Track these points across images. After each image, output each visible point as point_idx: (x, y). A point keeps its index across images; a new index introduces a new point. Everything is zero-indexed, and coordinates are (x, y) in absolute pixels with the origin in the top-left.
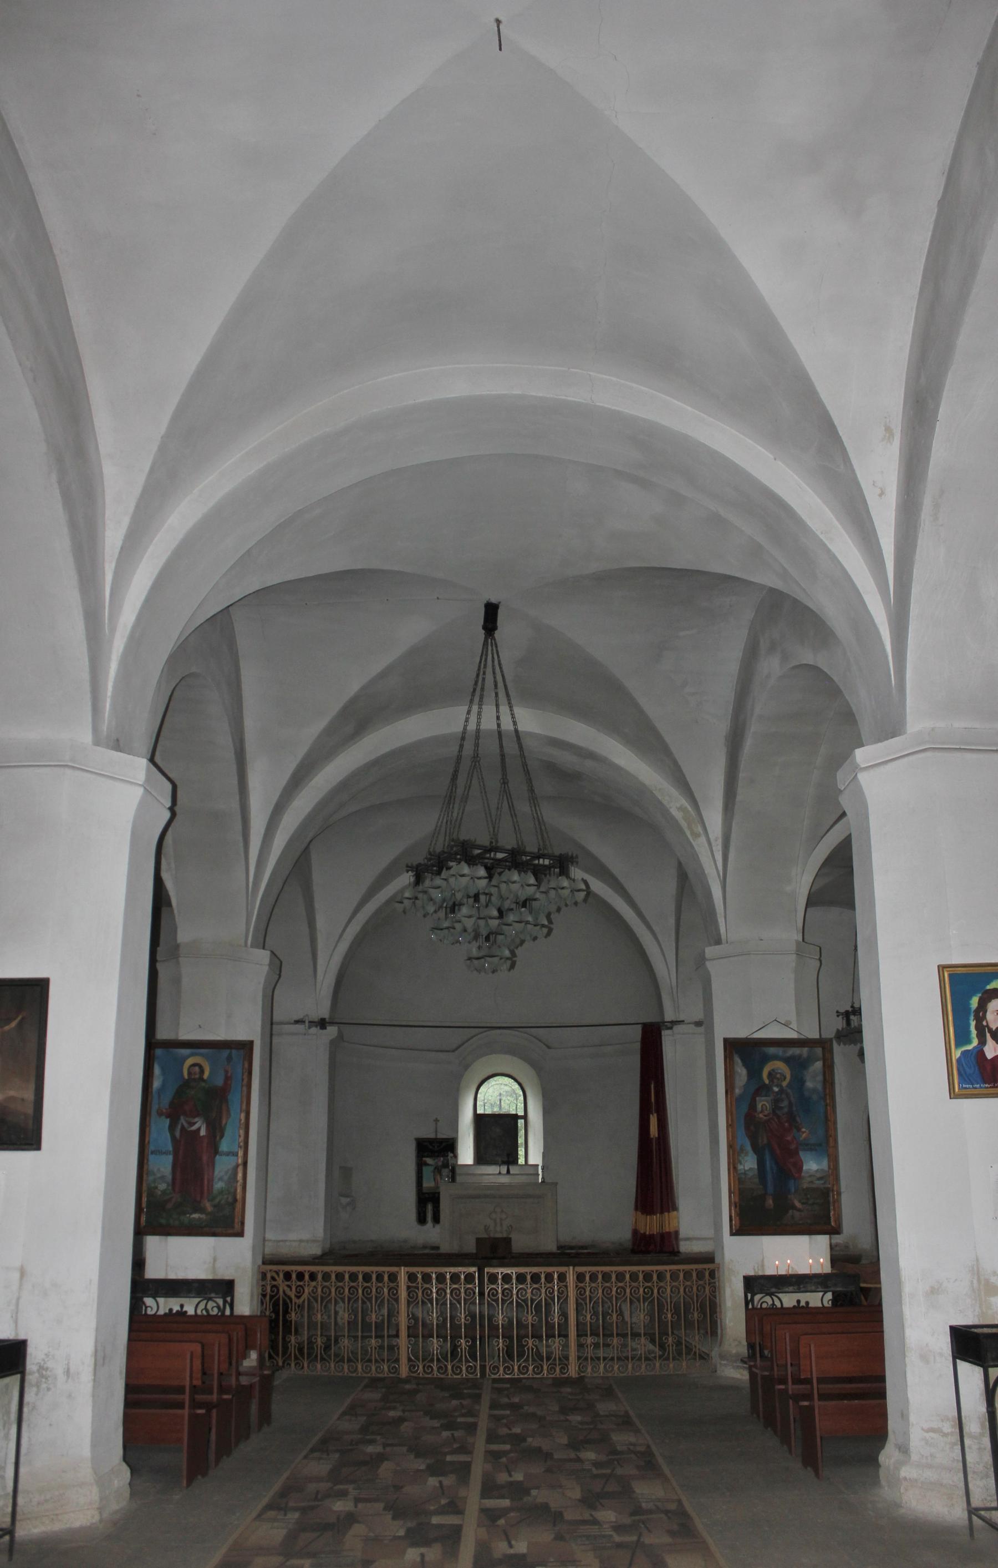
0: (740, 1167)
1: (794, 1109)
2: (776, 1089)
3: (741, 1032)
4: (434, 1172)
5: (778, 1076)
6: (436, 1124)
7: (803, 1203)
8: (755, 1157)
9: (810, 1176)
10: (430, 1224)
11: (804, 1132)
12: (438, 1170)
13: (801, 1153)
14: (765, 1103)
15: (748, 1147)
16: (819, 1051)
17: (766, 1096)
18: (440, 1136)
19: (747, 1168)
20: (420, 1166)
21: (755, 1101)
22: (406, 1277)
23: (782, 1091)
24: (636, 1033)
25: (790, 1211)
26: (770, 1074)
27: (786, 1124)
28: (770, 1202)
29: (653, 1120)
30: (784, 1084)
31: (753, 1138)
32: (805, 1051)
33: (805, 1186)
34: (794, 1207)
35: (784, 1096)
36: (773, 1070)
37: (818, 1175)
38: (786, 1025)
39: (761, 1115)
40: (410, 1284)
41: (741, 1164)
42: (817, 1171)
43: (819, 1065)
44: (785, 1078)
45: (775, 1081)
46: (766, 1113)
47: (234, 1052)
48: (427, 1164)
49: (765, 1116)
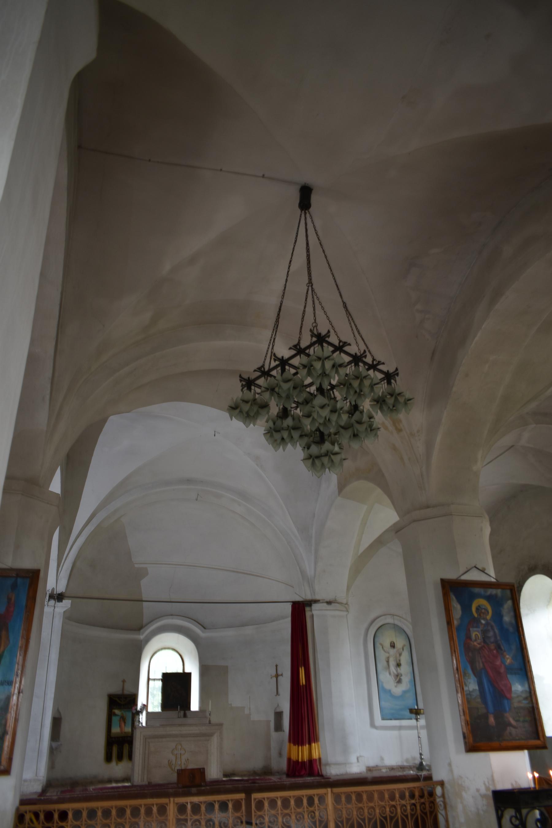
0: (466, 688)
1: (498, 638)
2: (483, 622)
3: (451, 575)
4: (120, 721)
5: (483, 611)
6: (123, 684)
7: (517, 721)
8: (476, 679)
9: (518, 697)
10: (114, 763)
11: (508, 659)
12: (123, 719)
13: (509, 676)
14: (477, 633)
15: (470, 671)
16: (508, 592)
17: (476, 627)
18: (126, 692)
19: (471, 689)
20: (110, 715)
21: (469, 630)
22: (176, 809)
23: (487, 624)
24: (288, 608)
25: (508, 728)
26: (478, 609)
27: (495, 651)
28: (492, 720)
29: (302, 671)
30: (489, 617)
31: (472, 663)
32: (499, 592)
33: (516, 705)
34: (510, 725)
35: (490, 628)
36: (479, 606)
37: (524, 695)
38: (483, 571)
39: (475, 643)
40: (180, 817)
41: (466, 685)
42: (522, 692)
43: (510, 603)
44: (488, 613)
45: (482, 615)
46: (479, 641)
47: (19, 580)
48: (115, 715)
49: (479, 644)
